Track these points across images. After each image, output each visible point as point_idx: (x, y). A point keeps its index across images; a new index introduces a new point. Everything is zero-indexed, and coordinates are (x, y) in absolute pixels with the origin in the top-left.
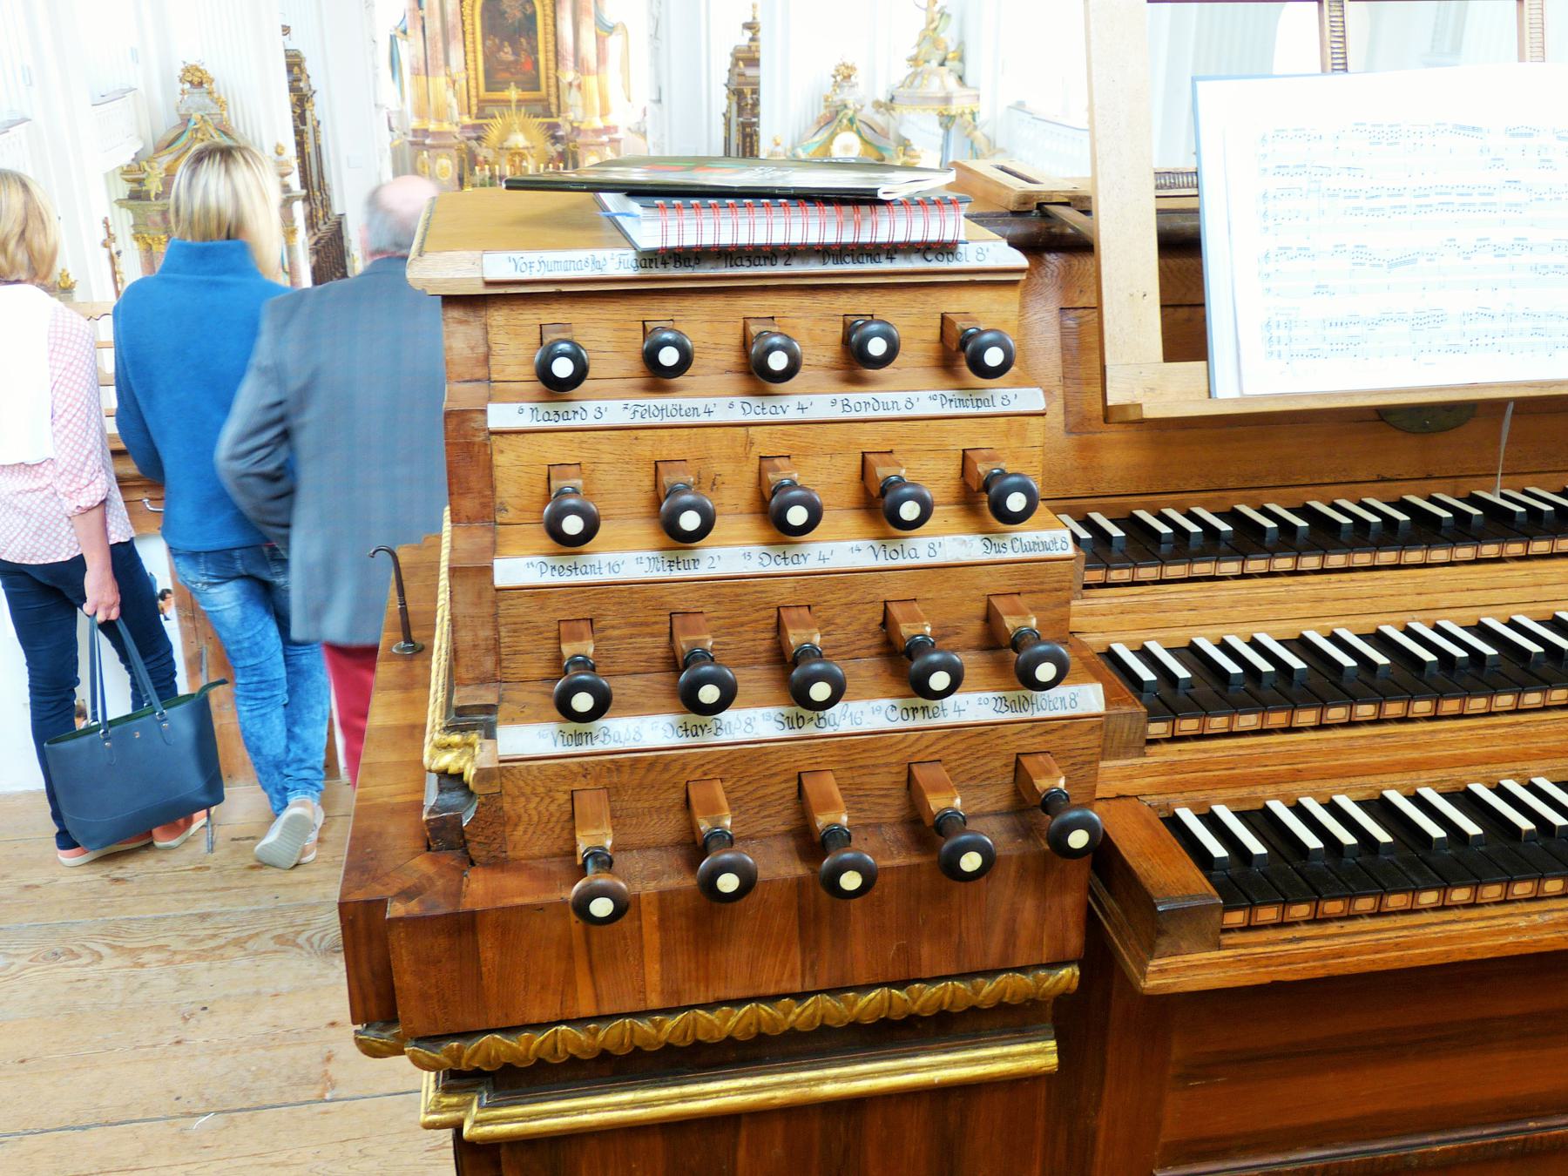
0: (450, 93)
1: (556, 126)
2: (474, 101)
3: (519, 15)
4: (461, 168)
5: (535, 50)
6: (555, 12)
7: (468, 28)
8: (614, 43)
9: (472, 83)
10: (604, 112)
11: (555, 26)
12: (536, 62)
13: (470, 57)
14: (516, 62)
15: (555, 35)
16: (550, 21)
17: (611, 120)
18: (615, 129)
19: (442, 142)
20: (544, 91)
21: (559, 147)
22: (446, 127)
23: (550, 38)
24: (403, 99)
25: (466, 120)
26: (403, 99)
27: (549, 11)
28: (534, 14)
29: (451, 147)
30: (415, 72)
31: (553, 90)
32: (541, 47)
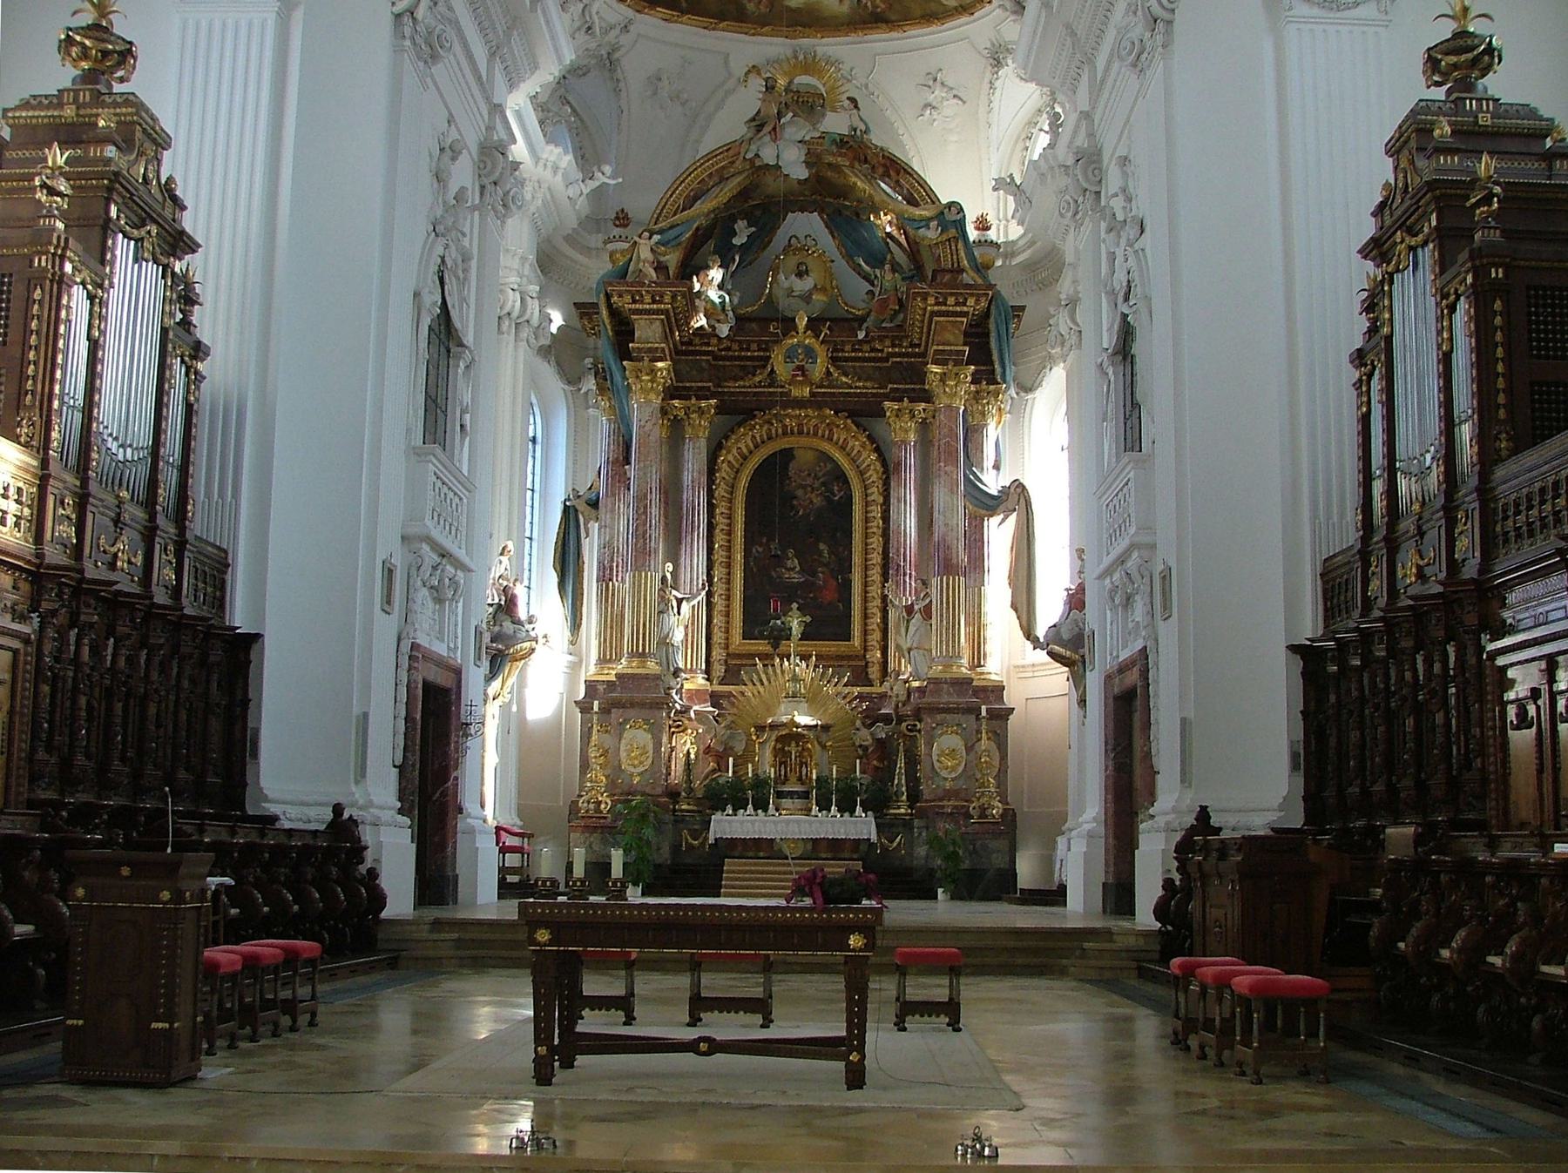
2: (717, 654)
3: (818, 501)
5: (845, 566)
6: (887, 498)
7: (720, 520)
8: (999, 534)
10: (978, 659)
11: (886, 518)
12: (847, 586)
13: (718, 573)
14: (807, 586)
15: (886, 534)
16: (876, 512)
18: (999, 689)
19: (638, 696)
21: (881, 731)
22: (652, 666)
23: (876, 542)
27: (876, 495)
31: (875, 637)
32: (857, 559)
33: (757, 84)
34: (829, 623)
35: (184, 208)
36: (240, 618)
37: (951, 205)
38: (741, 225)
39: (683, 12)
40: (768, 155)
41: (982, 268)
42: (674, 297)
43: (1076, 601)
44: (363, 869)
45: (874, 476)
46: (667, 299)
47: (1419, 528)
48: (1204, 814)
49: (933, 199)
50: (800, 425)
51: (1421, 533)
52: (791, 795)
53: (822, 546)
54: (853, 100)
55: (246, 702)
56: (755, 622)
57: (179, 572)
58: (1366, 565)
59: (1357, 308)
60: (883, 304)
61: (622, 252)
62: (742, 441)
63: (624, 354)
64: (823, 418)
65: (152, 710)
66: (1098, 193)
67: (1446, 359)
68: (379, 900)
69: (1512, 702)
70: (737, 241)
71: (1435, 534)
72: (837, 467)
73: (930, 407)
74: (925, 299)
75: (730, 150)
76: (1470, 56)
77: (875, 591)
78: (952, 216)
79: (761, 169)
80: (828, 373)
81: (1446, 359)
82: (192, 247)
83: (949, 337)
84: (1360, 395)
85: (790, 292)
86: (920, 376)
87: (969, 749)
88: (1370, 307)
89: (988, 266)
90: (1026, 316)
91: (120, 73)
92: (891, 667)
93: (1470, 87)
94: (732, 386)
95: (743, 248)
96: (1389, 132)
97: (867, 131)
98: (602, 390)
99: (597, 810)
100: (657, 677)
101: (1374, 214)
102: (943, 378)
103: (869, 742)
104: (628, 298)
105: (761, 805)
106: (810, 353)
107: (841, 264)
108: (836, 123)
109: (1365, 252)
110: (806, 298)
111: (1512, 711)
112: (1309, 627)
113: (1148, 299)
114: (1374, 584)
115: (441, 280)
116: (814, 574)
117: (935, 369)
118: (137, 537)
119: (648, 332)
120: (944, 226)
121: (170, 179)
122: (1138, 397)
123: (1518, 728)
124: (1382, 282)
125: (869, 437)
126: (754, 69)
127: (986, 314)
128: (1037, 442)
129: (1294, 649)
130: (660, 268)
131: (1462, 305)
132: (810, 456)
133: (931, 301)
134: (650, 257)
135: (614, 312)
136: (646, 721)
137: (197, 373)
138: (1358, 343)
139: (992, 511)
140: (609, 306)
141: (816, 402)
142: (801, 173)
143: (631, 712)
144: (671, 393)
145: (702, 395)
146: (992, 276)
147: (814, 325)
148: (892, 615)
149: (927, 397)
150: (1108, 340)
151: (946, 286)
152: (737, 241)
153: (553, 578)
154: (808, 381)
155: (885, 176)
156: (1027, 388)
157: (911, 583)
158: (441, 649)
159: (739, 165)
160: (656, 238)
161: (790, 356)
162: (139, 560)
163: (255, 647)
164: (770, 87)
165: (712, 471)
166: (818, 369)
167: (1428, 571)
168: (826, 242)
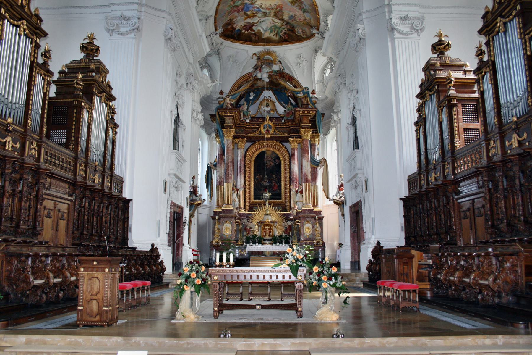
0: (235, 195)
1: (290, 214)
2: (247, 204)
3: (272, 164)
4: (237, 230)
8: (320, 171)
9: (247, 195)
10: (315, 204)
11: (290, 168)
12: (280, 186)
13: (247, 183)
15: (290, 173)
16: (287, 167)
17: (319, 208)
18: (320, 212)
20: (283, 200)
21: (290, 223)
23: (288, 175)
24: (211, 196)
25: (243, 211)
26: (211, 196)
27: (287, 163)
28: (280, 163)
29: (232, 217)
30: (219, 184)
31: (288, 199)
32: (283, 179)
33: (255, 58)
34: (276, 195)
35: (112, 89)
36: (126, 195)
37: (306, 88)
38: (252, 94)
39: (236, 40)
40: (259, 75)
41: (314, 103)
42: (235, 112)
43: (340, 187)
44: (159, 261)
45: (287, 157)
46: (234, 113)
47: (435, 167)
48: (379, 243)
49: (300, 86)
50: (267, 145)
51: (435, 168)
52: (268, 240)
53: (274, 176)
54: (280, 61)
55: (128, 217)
56: (257, 196)
57: (111, 183)
58: (420, 177)
59: (416, 111)
60: (288, 113)
61: (222, 101)
62: (253, 149)
63: (223, 127)
64: (273, 143)
65: (104, 220)
66: (345, 84)
67: (441, 124)
68: (163, 269)
69: (463, 212)
70: (251, 98)
71: (439, 168)
72: (277, 155)
73: (301, 140)
74: (299, 111)
75: (250, 74)
76: (443, 46)
77: (288, 187)
78: (305, 91)
79: (256, 79)
80: (275, 131)
81: (441, 124)
82: (115, 99)
83: (306, 121)
84: (417, 133)
85: (264, 111)
86: (298, 131)
87: (313, 227)
88: (418, 111)
89: (315, 103)
90: (325, 116)
91: (96, 55)
92: (292, 206)
93: (443, 54)
94: (250, 135)
95: (253, 100)
96: (423, 65)
97: (284, 69)
98: (217, 136)
99: (218, 244)
100: (232, 210)
101: (419, 87)
102: (305, 132)
103: (287, 226)
104: (223, 113)
105: (260, 242)
106: (270, 126)
107: (277, 104)
108: (276, 67)
109: (417, 96)
110: (269, 112)
111: (462, 214)
112: (405, 193)
113: (360, 110)
114: (422, 182)
115: (177, 108)
116: (271, 183)
117: (303, 130)
118: (100, 174)
119: (229, 121)
120: (304, 93)
121: (108, 81)
122: (358, 135)
123: (464, 219)
124: (422, 104)
125: (285, 148)
126: (255, 54)
127: (315, 116)
128: (330, 148)
129: (401, 199)
130: (231, 105)
131: (445, 109)
132: (270, 153)
133: (301, 112)
134: (229, 102)
135: (220, 116)
136: (230, 222)
137: (115, 131)
138: (416, 120)
139: (318, 166)
140: (219, 114)
141: (271, 139)
142: (267, 80)
143: (226, 219)
144: (234, 137)
145: (243, 137)
146: (317, 106)
147: (271, 119)
148: (292, 193)
149: (300, 137)
150: (349, 121)
151: (305, 108)
152: (251, 98)
153: (205, 185)
154: (270, 134)
155: (288, 81)
156: (325, 134)
157: (297, 185)
158: (178, 203)
159: (251, 78)
160: (230, 97)
161: (264, 128)
162: (101, 180)
163: (131, 202)
164: (259, 58)
165: (245, 157)
166: (271, 131)
167: (437, 178)
168: (274, 98)
